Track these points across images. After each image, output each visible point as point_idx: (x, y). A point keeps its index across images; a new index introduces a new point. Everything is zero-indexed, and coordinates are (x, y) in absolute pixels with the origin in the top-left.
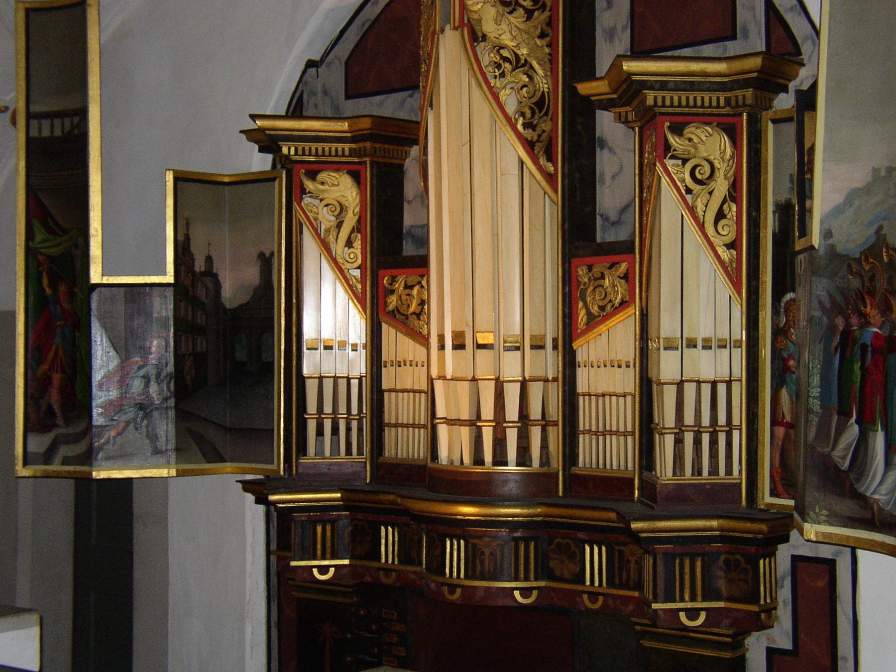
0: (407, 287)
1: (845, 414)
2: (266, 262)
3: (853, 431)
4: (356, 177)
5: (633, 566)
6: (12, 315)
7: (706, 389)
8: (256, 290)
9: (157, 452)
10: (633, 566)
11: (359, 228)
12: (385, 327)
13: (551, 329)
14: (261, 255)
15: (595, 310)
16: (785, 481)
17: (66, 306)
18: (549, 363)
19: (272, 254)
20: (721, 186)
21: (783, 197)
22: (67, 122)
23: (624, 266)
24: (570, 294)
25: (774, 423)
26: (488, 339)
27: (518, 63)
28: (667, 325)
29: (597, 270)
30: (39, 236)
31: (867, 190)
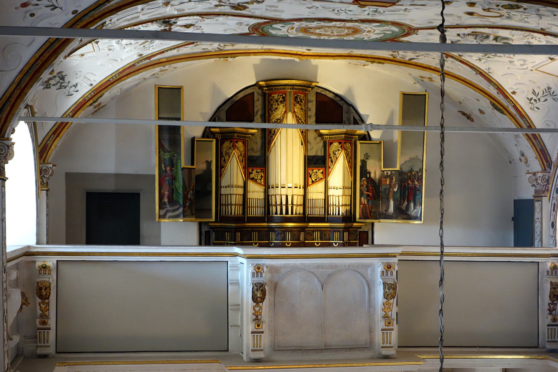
0: (257, 172)
1: (404, 200)
2: (209, 163)
3: (406, 203)
5: (328, 236)
6: (155, 175)
7: (337, 198)
8: (204, 171)
9: (192, 215)
10: (328, 236)
12: (249, 182)
13: (302, 184)
14: (207, 161)
15: (314, 180)
16: (364, 216)
17: (169, 173)
18: (301, 191)
19: (211, 161)
21: (362, 159)
23: (321, 171)
24: (307, 176)
25: (360, 204)
26: (290, 185)
29: (314, 171)
30: (162, 153)
31: (409, 161)
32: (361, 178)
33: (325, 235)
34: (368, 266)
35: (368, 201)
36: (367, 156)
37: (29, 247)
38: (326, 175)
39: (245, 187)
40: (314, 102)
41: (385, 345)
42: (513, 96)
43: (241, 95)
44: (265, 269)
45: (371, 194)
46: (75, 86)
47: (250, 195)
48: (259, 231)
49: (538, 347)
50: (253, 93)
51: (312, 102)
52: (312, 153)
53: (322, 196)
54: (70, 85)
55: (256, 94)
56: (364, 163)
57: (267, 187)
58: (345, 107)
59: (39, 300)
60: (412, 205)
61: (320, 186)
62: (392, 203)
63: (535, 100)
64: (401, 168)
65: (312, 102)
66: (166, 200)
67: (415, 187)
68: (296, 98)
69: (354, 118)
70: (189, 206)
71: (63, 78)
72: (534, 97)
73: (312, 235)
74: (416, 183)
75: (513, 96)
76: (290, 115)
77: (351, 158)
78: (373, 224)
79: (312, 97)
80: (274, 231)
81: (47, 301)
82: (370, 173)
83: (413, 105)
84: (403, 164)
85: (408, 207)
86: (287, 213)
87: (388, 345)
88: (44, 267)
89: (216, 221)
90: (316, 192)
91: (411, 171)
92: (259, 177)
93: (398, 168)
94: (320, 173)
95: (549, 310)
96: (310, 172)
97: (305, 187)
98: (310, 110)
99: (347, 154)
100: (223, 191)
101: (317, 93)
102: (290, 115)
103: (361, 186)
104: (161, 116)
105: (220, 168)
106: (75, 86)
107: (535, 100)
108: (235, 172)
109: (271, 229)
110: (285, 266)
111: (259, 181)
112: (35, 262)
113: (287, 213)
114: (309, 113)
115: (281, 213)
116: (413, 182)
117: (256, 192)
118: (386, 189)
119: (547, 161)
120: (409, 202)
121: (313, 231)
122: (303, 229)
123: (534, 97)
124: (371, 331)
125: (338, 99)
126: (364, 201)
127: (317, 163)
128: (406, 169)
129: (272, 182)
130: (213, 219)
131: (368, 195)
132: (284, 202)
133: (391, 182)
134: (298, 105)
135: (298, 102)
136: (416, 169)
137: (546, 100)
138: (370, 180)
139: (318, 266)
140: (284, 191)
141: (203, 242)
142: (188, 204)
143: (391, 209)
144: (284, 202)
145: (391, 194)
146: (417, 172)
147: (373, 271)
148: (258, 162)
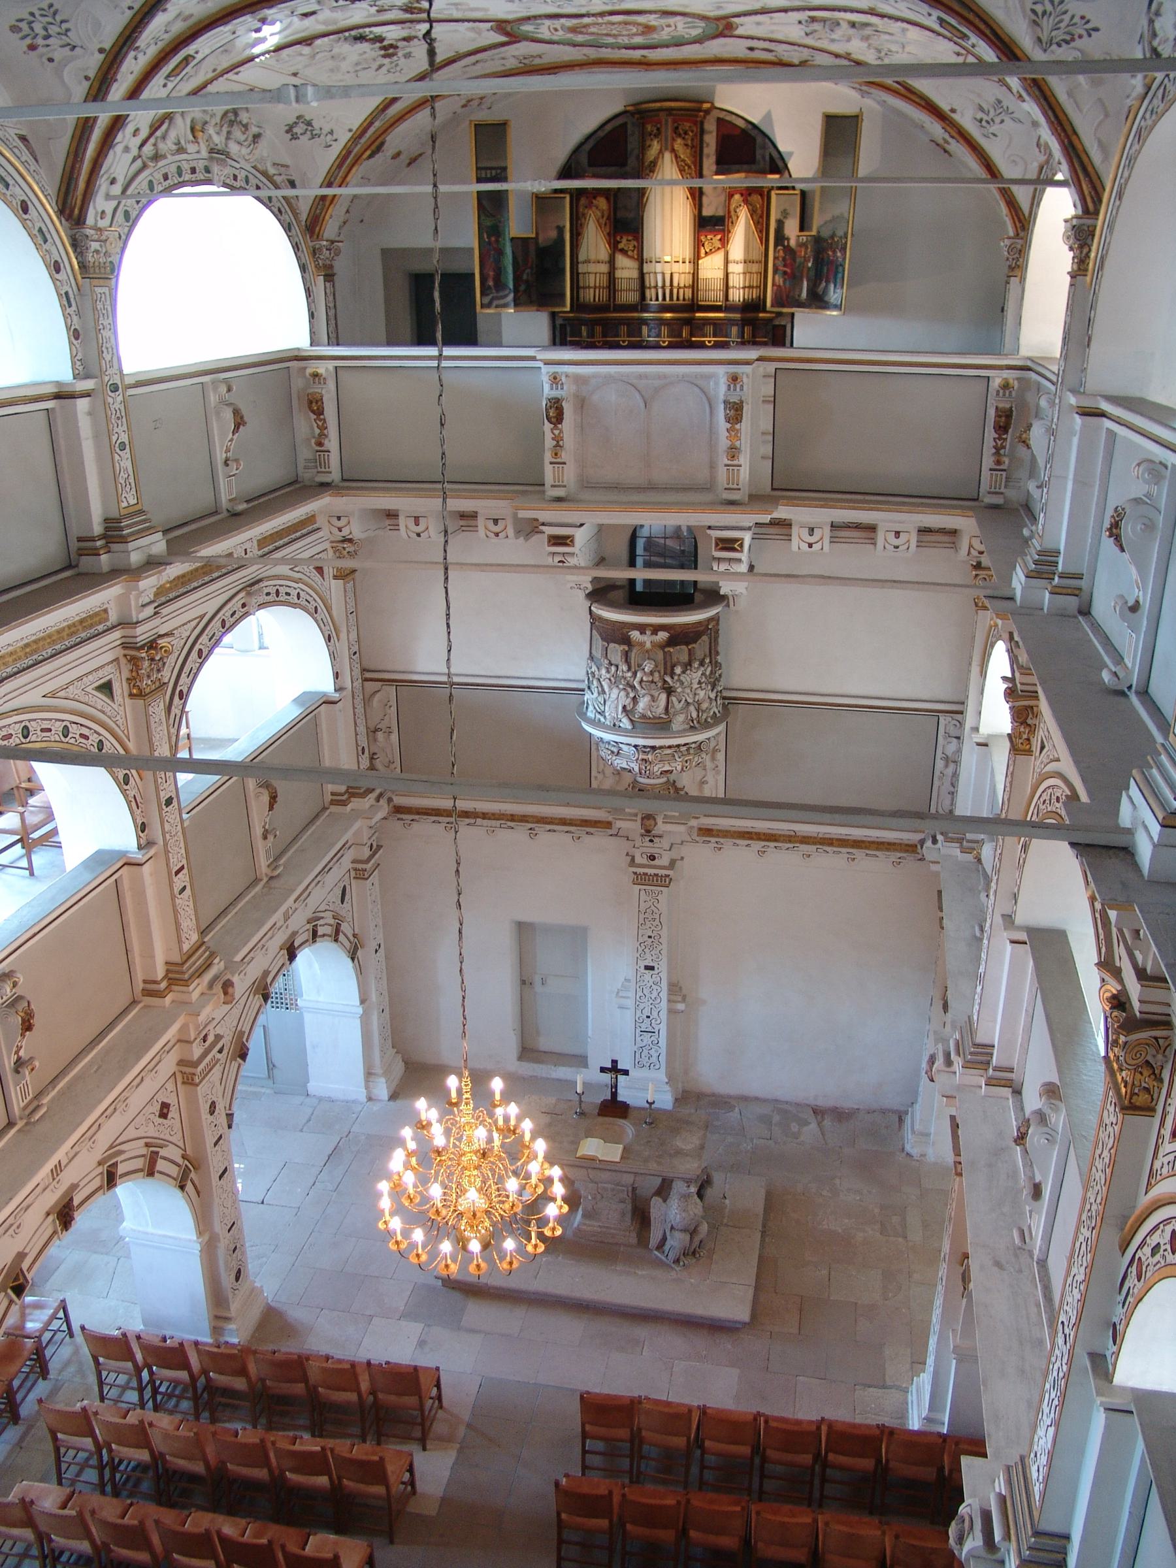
2: (561, 230)
4: (608, 199)
11: (608, 218)
16: (778, 302)
18: (687, 268)
20: (759, 212)
22: (494, 172)
23: (719, 237)
24: (698, 244)
25: (773, 285)
27: (689, 167)
28: (731, 258)
31: (830, 221)
32: (776, 246)
33: (721, 330)
34: (708, 377)
35: (784, 282)
37: (298, 349)
38: (724, 242)
39: (612, 262)
40: (715, 134)
41: (731, 486)
43: (609, 128)
44: (563, 379)
45: (788, 270)
46: (331, 133)
47: (619, 274)
48: (628, 325)
49: (977, 500)
50: (626, 123)
51: (710, 132)
52: (707, 212)
53: (720, 274)
54: (324, 132)
55: (629, 126)
56: (780, 224)
57: (641, 261)
58: (759, 140)
59: (313, 417)
60: (832, 286)
61: (717, 259)
62: (805, 283)
63: (988, 122)
64: (819, 232)
65: (710, 132)
66: (491, 283)
68: (677, 128)
69: (771, 157)
70: (525, 291)
71: (309, 124)
73: (702, 330)
76: (668, 156)
77: (761, 217)
78: (793, 315)
79: (711, 126)
80: (647, 324)
82: (788, 239)
86: (664, 299)
87: (735, 486)
88: (316, 375)
89: (572, 311)
90: (711, 267)
95: (995, 447)
96: (703, 238)
97: (696, 258)
98: (708, 145)
99: (753, 212)
100: (582, 268)
101: (719, 119)
102: (668, 156)
103: (775, 258)
104: (480, 165)
105: (576, 234)
106: (331, 133)
108: (595, 243)
109: (644, 322)
110: (595, 376)
111: (630, 253)
112: (305, 368)
113: (664, 299)
114: (706, 151)
115: (657, 299)
117: (626, 268)
119: (1020, 221)
121: (704, 325)
122: (689, 322)
124: (712, 466)
125: (750, 127)
126: (779, 280)
127: (709, 226)
128: (825, 234)
130: (568, 309)
131: (785, 273)
132: (660, 284)
134: (679, 141)
135: (680, 135)
138: (788, 249)
139: (640, 376)
141: (558, 340)
142: (522, 287)
143: (804, 294)
144: (660, 284)
147: (717, 383)
148: (627, 224)
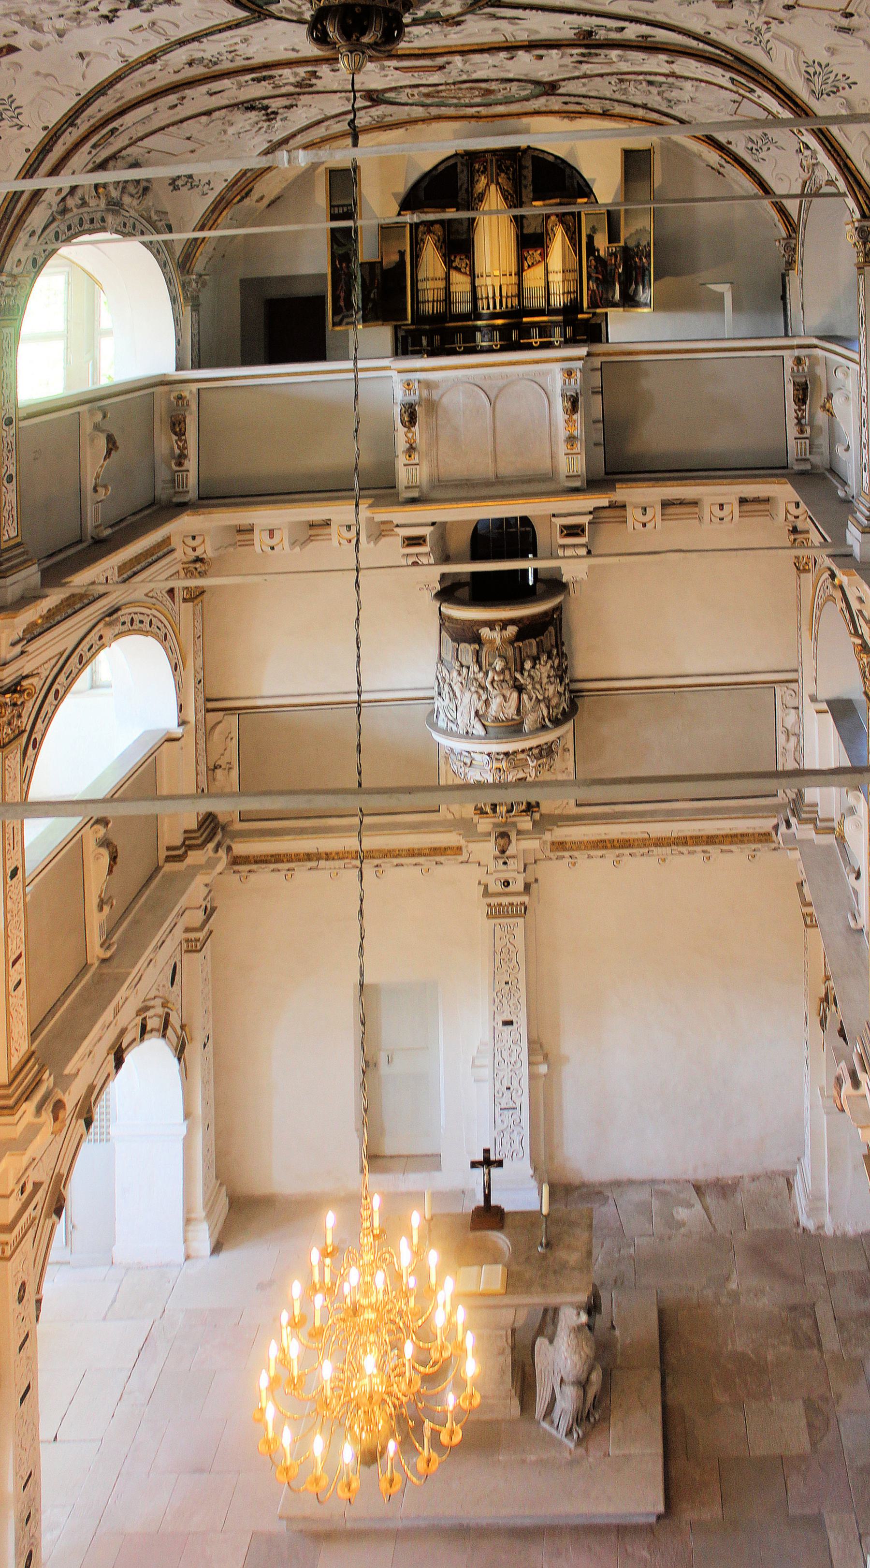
36: (594, 230)
42: (729, 146)
67: (643, 266)
72: (755, 147)
74: (644, 260)
75: (729, 146)
81: (183, 438)
83: (635, 163)
84: (628, 238)
85: (636, 291)
91: (638, 246)
92: (464, 265)
93: (622, 244)
94: (537, 254)
107: (757, 150)
108: (432, 262)
116: (641, 259)
118: (611, 270)
120: (637, 285)
123: (755, 147)
129: (477, 271)
132: (491, 295)
133: (616, 261)
136: (644, 243)
137: (769, 149)
140: (489, 281)
143: (617, 296)
145: (616, 276)
146: (645, 247)
